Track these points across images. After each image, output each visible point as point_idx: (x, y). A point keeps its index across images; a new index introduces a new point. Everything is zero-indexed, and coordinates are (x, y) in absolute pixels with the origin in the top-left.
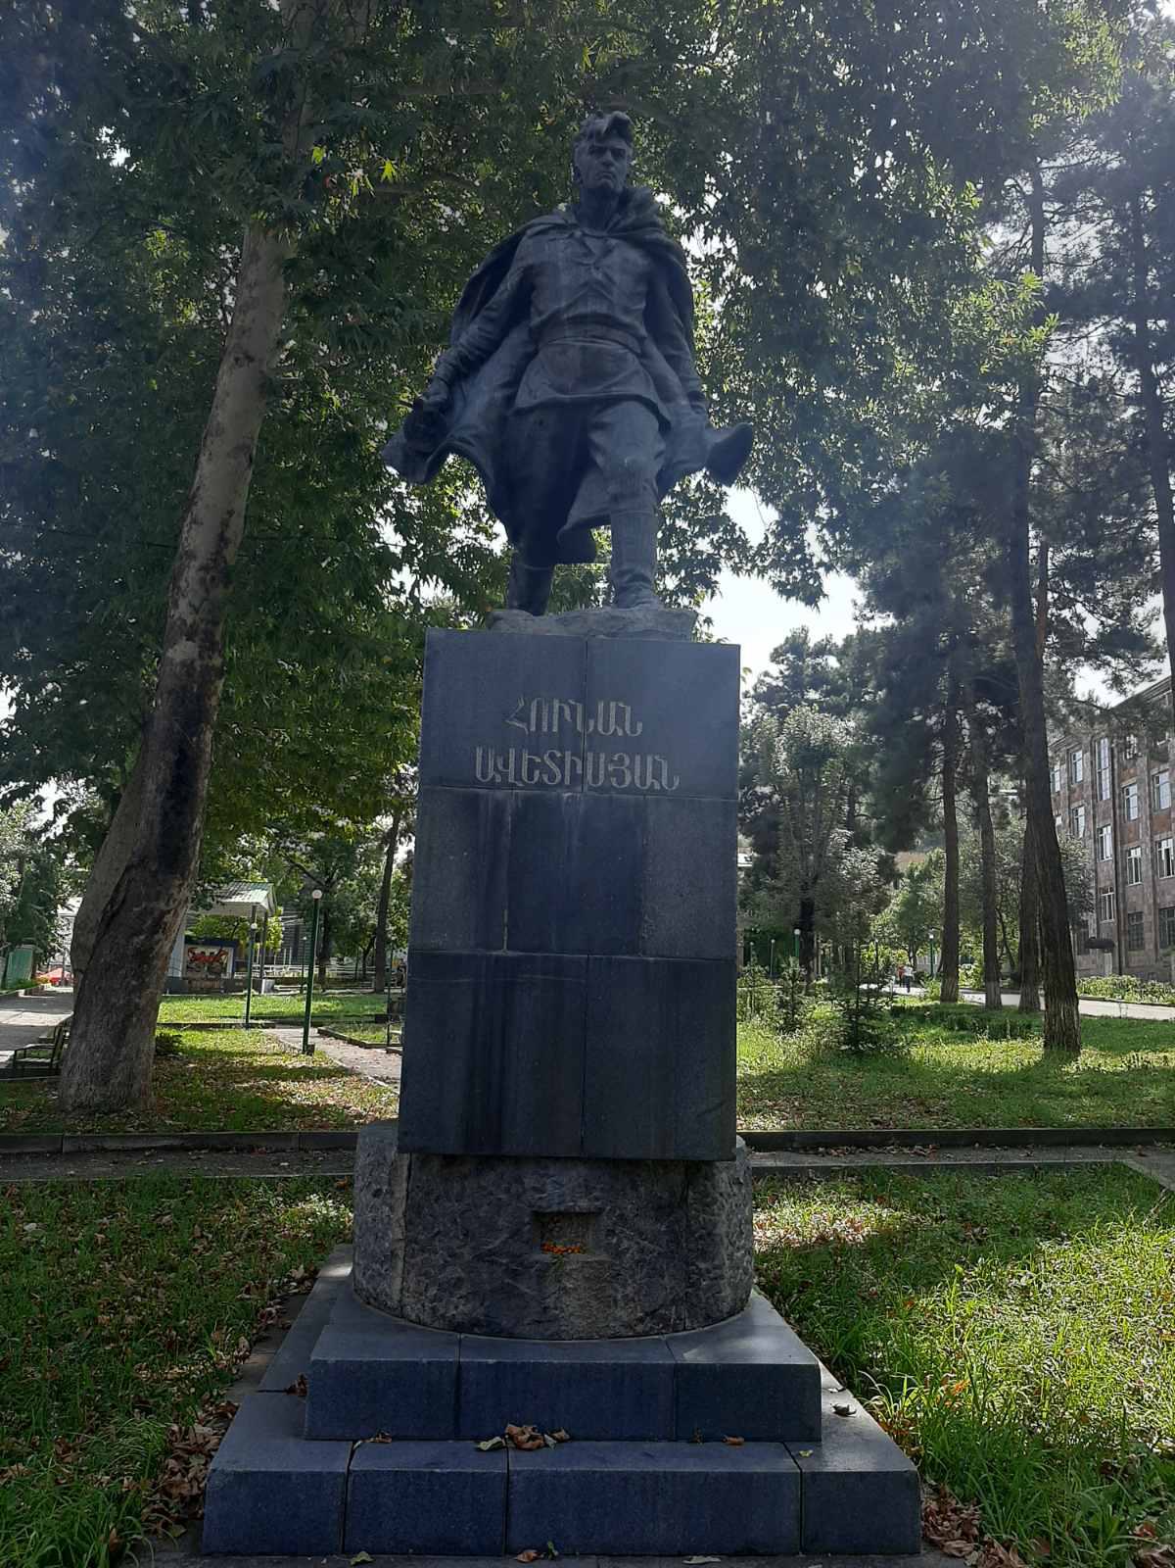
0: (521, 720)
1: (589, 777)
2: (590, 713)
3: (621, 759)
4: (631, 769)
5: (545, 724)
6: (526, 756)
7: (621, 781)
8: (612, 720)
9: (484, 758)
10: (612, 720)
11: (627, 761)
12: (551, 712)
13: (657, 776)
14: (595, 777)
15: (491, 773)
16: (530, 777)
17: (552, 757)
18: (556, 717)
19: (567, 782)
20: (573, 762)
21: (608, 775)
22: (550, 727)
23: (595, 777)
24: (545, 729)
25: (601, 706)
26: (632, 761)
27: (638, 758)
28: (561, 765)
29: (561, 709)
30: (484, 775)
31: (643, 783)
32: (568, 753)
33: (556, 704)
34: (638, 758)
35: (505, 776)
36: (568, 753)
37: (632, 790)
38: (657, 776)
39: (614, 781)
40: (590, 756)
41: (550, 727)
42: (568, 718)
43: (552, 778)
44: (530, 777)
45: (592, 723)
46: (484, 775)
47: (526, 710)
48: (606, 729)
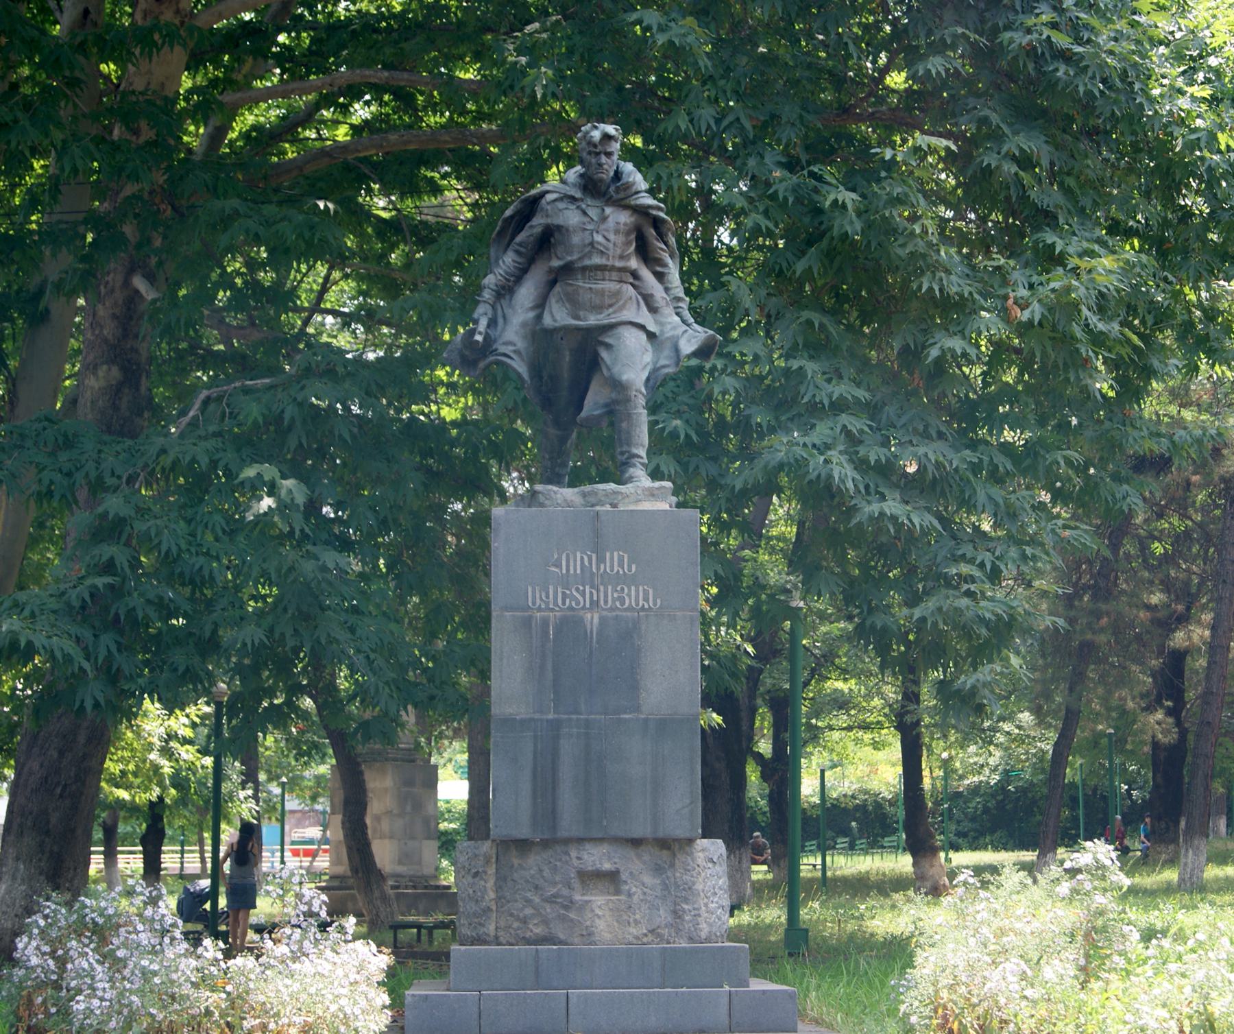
0: (556, 566)
1: (602, 602)
2: (601, 560)
3: (622, 589)
4: (629, 595)
5: (572, 568)
6: (560, 590)
7: (623, 603)
8: (616, 564)
9: (534, 592)
10: (616, 564)
11: (626, 590)
12: (575, 561)
13: (646, 599)
14: (606, 602)
15: (538, 602)
16: (564, 603)
17: (577, 590)
18: (579, 563)
19: (588, 605)
20: (591, 593)
21: (614, 600)
22: (575, 570)
23: (606, 602)
24: (572, 572)
25: (608, 555)
26: (630, 590)
27: (633, 588)
28: (584, 595)
29: (582, 559)
30: (534, 603)
31: (637, 604)
32: (587, 587)
33: (579, 555)
34: (633, 588)
35: (547, 604)
36: (587, 587)
37: (630, 609)
38: (646, 599)
39: (618, 604)
40: (602, 588)
41: (575, 570)
42: (586, 563)
43: (578, 603)
44: (564, 603)
45: (602, 566)
46: (534, 603)
47: (560, 559)
48: (612, 570)
